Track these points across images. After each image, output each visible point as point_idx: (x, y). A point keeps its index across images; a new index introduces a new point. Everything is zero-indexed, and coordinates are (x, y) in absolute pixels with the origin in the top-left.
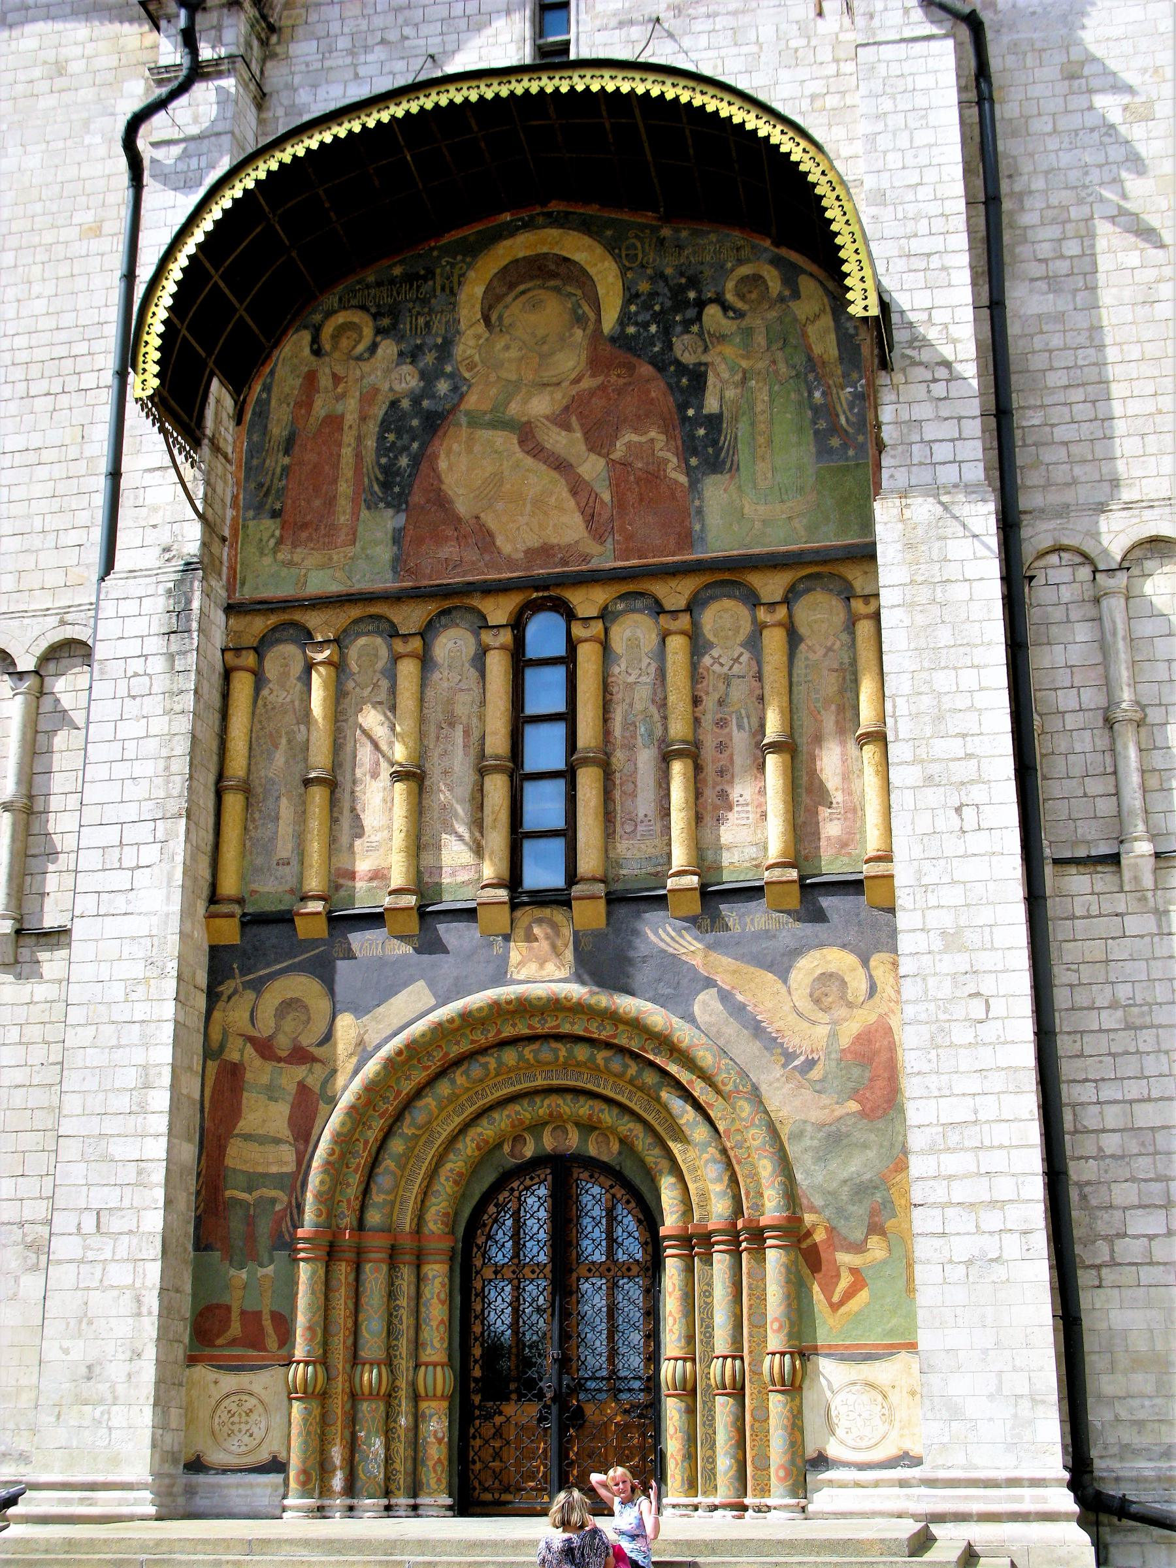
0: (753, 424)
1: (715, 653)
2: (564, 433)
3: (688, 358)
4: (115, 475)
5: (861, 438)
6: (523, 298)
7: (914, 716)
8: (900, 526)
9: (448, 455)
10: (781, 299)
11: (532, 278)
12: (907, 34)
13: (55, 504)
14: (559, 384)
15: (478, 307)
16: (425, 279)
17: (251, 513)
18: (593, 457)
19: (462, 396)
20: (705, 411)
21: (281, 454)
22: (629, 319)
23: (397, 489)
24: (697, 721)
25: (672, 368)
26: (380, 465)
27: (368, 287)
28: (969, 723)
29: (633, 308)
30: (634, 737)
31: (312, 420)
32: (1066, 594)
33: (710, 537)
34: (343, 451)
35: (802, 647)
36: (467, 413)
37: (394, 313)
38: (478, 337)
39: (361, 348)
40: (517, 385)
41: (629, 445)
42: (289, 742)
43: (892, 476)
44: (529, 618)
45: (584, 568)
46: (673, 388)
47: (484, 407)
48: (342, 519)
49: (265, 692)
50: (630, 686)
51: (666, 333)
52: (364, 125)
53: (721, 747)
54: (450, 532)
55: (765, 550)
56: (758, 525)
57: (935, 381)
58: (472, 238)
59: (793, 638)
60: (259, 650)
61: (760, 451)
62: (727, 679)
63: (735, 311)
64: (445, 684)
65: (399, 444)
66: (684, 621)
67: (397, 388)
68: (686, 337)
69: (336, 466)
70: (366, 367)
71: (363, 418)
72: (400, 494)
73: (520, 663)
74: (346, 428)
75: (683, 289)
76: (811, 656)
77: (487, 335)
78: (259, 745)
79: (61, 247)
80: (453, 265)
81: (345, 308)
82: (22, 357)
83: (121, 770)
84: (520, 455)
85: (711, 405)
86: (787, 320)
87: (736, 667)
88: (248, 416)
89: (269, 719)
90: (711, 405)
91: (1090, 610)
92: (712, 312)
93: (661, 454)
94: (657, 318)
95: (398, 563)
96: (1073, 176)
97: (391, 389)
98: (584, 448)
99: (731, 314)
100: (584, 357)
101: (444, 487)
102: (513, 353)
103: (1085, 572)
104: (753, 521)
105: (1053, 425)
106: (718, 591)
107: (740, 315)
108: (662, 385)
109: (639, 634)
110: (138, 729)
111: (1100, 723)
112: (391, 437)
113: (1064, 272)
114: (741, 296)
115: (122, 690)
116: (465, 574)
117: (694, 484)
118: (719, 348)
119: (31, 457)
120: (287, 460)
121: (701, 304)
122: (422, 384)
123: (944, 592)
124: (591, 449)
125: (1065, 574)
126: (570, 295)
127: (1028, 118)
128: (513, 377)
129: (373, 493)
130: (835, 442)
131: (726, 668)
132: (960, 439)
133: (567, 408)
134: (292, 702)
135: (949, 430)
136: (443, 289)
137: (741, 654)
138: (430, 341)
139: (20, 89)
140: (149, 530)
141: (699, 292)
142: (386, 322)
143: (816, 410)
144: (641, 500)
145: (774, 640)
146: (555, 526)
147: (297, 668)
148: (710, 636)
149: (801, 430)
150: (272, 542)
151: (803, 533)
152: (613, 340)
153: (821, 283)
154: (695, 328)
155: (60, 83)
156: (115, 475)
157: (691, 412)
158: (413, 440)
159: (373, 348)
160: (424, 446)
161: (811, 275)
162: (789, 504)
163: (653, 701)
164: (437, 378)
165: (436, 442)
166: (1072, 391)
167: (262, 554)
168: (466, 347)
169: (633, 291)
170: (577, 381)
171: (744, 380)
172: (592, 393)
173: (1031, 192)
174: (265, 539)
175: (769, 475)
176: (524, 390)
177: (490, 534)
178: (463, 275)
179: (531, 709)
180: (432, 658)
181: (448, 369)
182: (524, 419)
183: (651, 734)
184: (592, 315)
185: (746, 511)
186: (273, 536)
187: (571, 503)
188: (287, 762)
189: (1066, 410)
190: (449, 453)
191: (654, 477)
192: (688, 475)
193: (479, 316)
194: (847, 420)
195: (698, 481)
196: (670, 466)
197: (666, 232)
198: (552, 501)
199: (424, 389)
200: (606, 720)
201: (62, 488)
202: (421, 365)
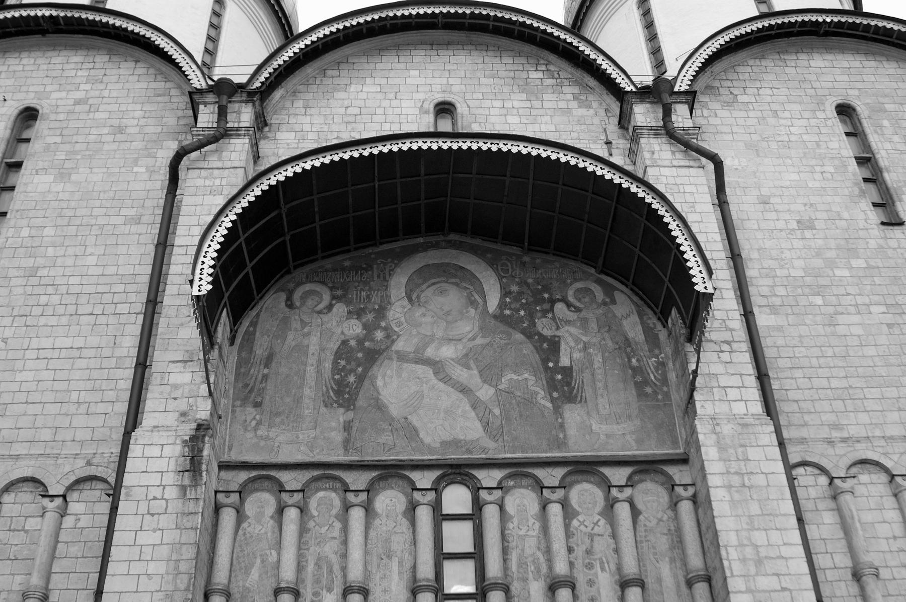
0: (593, 375)
1: (581, 518)
2: (465, 370)
3: (547, 332)
4: (142, 365)
5: (665, 389)
6: (434, 287)
7: (743, 560)
8: (714, 436)
9: (384, 377)
10: (604, 303)
11: (439, 277)
12: (675, 163)
13: (89, 385)
14: (460, 340)
15: (403, 289)
16: (366, 270)
17: (238, 403)
18: (486, 386)
19: (393, 342)
20: (561, 364)
21: (262, 367)
22: (506, 306)
23: (347, 396)
24: (571, 564)
25: (536, 337)
26: (333, 378)
27: (327, 271)
28: (780, 566)
29: (508, 300)
30: (526, 572)
31: (285, 347)
32: (813, 493)
33: (571, 442)
34: (308, 368)
35: (641, 517)
36: (397, 352)
37: (345, 288)
38: (404, 307)
39: (321, 306)
40: (432, 338)
41: (510, 380)
42: (263, 561)
43: (702, 406)
44: (444, 488)
45: (484, 456)
46: (538, 349)
47: (408, 350)
48: (306, 412)
49: (245, 525)
50: (522, 538)
51: (531, 316)
52: (361, 154)
53: (591, 583)
54: (385, 426)
55: (609, 453)
56: (602, 437)
57: (722, 352)
58: (398, 250)
59: (635, 512)
60: (241, 492)
61: (600, 392)
62: (591, 536)
63: (575, 307)
64: (385, 528)
65: (348, 367)
66: (560, 493)
67: (346, 331)
68: (544, 319)
69: (303, 378)
70: (325, 318)
71: (322, 349)
72: (349, 400)
73: (440, 517)
74: (310, 354)
75: (541, 292)
76: (648, 524)
77: (410, 306)
78: (239, 563)
79: (109, 227)
80: (385, 264)
81: (310, 282)
82: (74, 290)
83: (137, 568)
84: (434, 381)
85: (564, 361)
86: (610, 315)
87: (596, 529)
88: (238, 341)
89: (247, 544)
90: (564, 361)
91: (832, 505)
92: (560, 307)
93: (532, 388)
94: (523, 306)
95: (347, 444)
96: (774, 253)
97: (342, 333)
98: (479, 380)
99: (573, 309)
100: (477, 325)
101: (380, 397)
102: (428, 319)
103: (823, 480)
104: (599, 434)
105: (786, 390)
106: (579, 477)
107: (578, 310)
108: (531, 346)
109: (525, 502)
110: (155, 538)
111: (850, 577)
112: (343, 363)
113: (779, 303)
114: (579, 300)
115: (143, 508)
116: (398, 454)
117: (557, 410)
118: (566, 328)
119: (76, 353)
120: (266, 371)
121: (553, 302)
122: (364, 332)
123: (749, 479)
124: (484, 382)
125: (810, 480)
126: (466, 288)
127: (742, 220)
128: (429, 334)
129: (329, 397)
130: (649, 390)
131: (589, 529)
132: (743, 387)
133: (466, 355)
134: (266, 533)
135: (736, 381)
136: (379, 277)
137: (599, 520)
138: (370, 306)
139: (92, 138)
140: (170, 401)
141: (551, 294)
142: (339, 293)
143: (634, 369)
144: (521, 416)
145: (623, 511)
146: (461, 427)
147: (271, 509)
148: (576, 507)
149: (625, 381)
150: (254, 423)
151: (633, 443)
152: (495, 317)
153: (628, 296)
154: (550, 315)
155: (119, 137)
156: (142, 365)
157: (551, 365)
158: (359, 366)
159: (330, 307)
160: (366, 371)
161: (622, 291)
162: (623, 425)
163: (539, 549)
164: (375, 329)
165: (375, 368)
166: (794, 371)
167: (246, 430)
168: (398, 311)
169: (507, 290)
170: (473, 339)
171: (585, 348)
172: (484, 347)
173: (751, 259)
174: (248, 420)
175: (607, 407)
176: (436, 342)
177: (415, 429)
178: (393, 270)
179: (448, 548)
180: (373, 509)
181: (383, 324)
182: (438, 359)
183: (538, 570)
184: (480, 300)
185: (594, 427)
186: (254, 419)
187: (473, 414)
188: (260, 576)
189: (793, 381)
190: (384, 377)
191: (529, 401)
192: (552, 402)
193: (404, 295)
194: (655, 377)
195: (559, 407)
196: (539, 396)
197: (526, 259)
198: (460, 410)
199: (366, 335)
200: (505, 560)
201: (95, 374)
202: (364, 320)
